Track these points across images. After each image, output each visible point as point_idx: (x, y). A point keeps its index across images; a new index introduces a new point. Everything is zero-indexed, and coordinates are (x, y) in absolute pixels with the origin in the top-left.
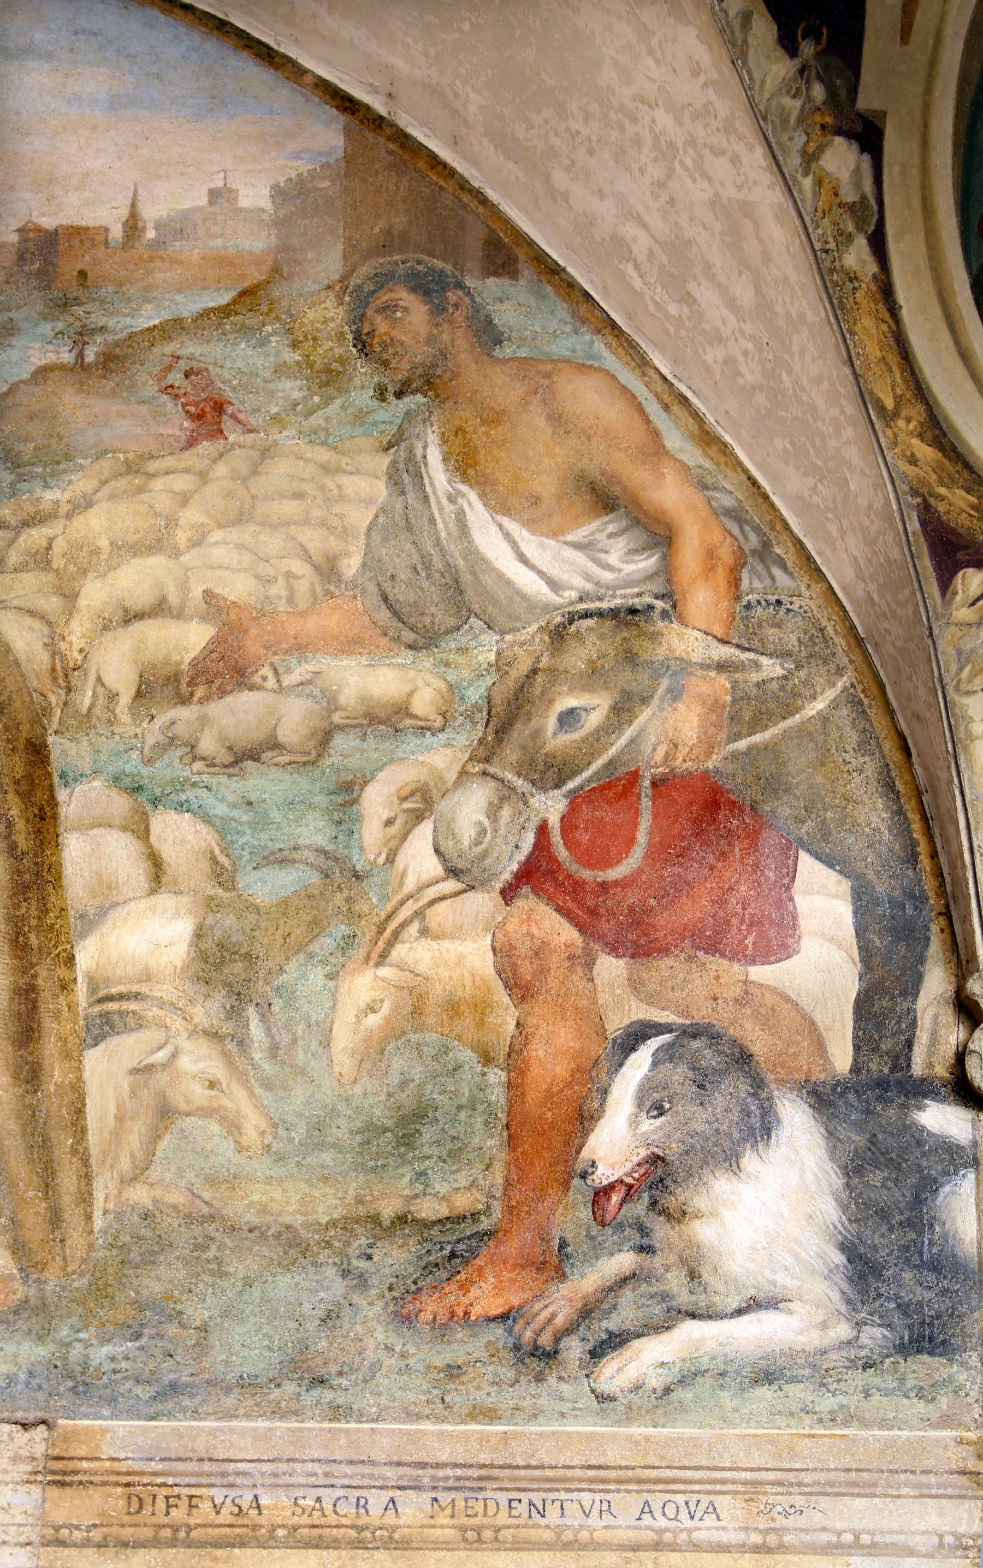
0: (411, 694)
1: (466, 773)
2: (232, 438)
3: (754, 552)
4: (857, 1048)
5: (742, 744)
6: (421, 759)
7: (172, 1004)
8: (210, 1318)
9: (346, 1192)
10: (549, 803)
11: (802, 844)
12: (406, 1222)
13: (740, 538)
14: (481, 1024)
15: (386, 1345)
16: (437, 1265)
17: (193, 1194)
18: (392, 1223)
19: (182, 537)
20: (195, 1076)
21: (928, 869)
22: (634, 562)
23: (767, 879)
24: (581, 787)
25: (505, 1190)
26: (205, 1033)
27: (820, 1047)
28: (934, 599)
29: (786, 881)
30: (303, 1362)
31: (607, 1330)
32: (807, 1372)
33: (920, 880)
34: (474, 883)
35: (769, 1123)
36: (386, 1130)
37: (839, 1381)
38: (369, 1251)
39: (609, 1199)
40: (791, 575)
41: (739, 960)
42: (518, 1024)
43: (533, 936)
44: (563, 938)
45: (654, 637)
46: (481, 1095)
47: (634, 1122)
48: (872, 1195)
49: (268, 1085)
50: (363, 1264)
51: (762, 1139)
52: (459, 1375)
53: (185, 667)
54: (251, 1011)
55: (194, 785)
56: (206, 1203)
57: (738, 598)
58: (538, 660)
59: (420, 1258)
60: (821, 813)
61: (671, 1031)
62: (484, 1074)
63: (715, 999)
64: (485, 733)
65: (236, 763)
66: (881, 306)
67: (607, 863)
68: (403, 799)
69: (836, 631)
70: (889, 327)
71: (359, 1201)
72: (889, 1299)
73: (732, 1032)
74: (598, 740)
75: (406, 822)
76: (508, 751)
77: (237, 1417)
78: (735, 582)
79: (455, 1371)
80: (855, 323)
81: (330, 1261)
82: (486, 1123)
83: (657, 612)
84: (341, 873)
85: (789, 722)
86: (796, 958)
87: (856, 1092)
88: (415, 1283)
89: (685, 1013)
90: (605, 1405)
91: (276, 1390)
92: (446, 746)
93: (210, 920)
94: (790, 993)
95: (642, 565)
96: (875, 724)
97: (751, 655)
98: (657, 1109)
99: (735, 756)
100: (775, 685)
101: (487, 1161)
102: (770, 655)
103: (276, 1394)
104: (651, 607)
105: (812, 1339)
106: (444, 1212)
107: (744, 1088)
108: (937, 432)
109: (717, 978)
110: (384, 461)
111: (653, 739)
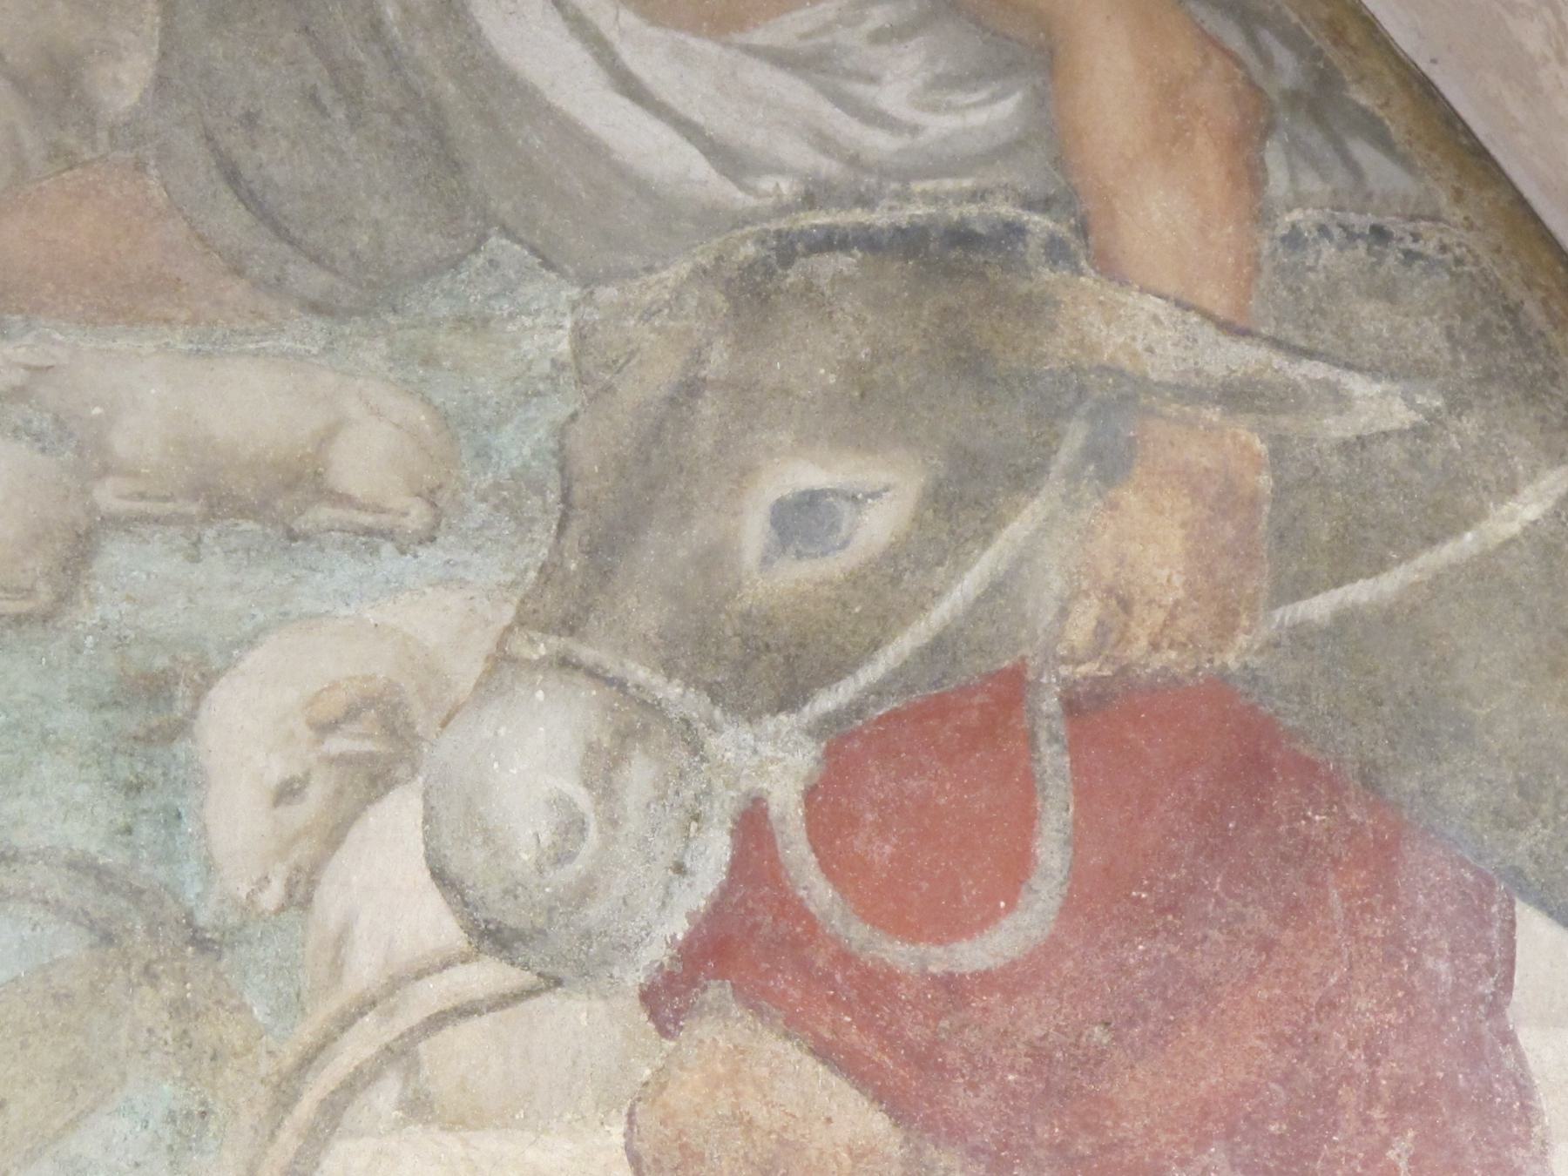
0: (328, 435)
1: (513, 660)
3: (1294, 98)
5: (1319, 607)
6: (371, 616)
10: (767, 750)
11: (1519, 884)
22: (951, 108)
23: (1432, 979)
24: (857, 709)
29: (1486, 987)
34: (563, 972)
40: (1404, 161)
43: (749, 1125)
45: (1035, 309)
57: (1262, 216)
58: (698, 357)
64: (557, 549)
68: (325, 728)
74: (895, 580)
75: (339, 792)
76: (632, 602)
78: (1252, 176)
83: (1033, 247)
84: (151, 931)
92: (444, 582)
95: (978, 118)
97: (1318, 370)
99: (1301, 638)
100: (1394, 452)
102: (1374, 371)
104: (1015, 231)
111: (1057, 583)
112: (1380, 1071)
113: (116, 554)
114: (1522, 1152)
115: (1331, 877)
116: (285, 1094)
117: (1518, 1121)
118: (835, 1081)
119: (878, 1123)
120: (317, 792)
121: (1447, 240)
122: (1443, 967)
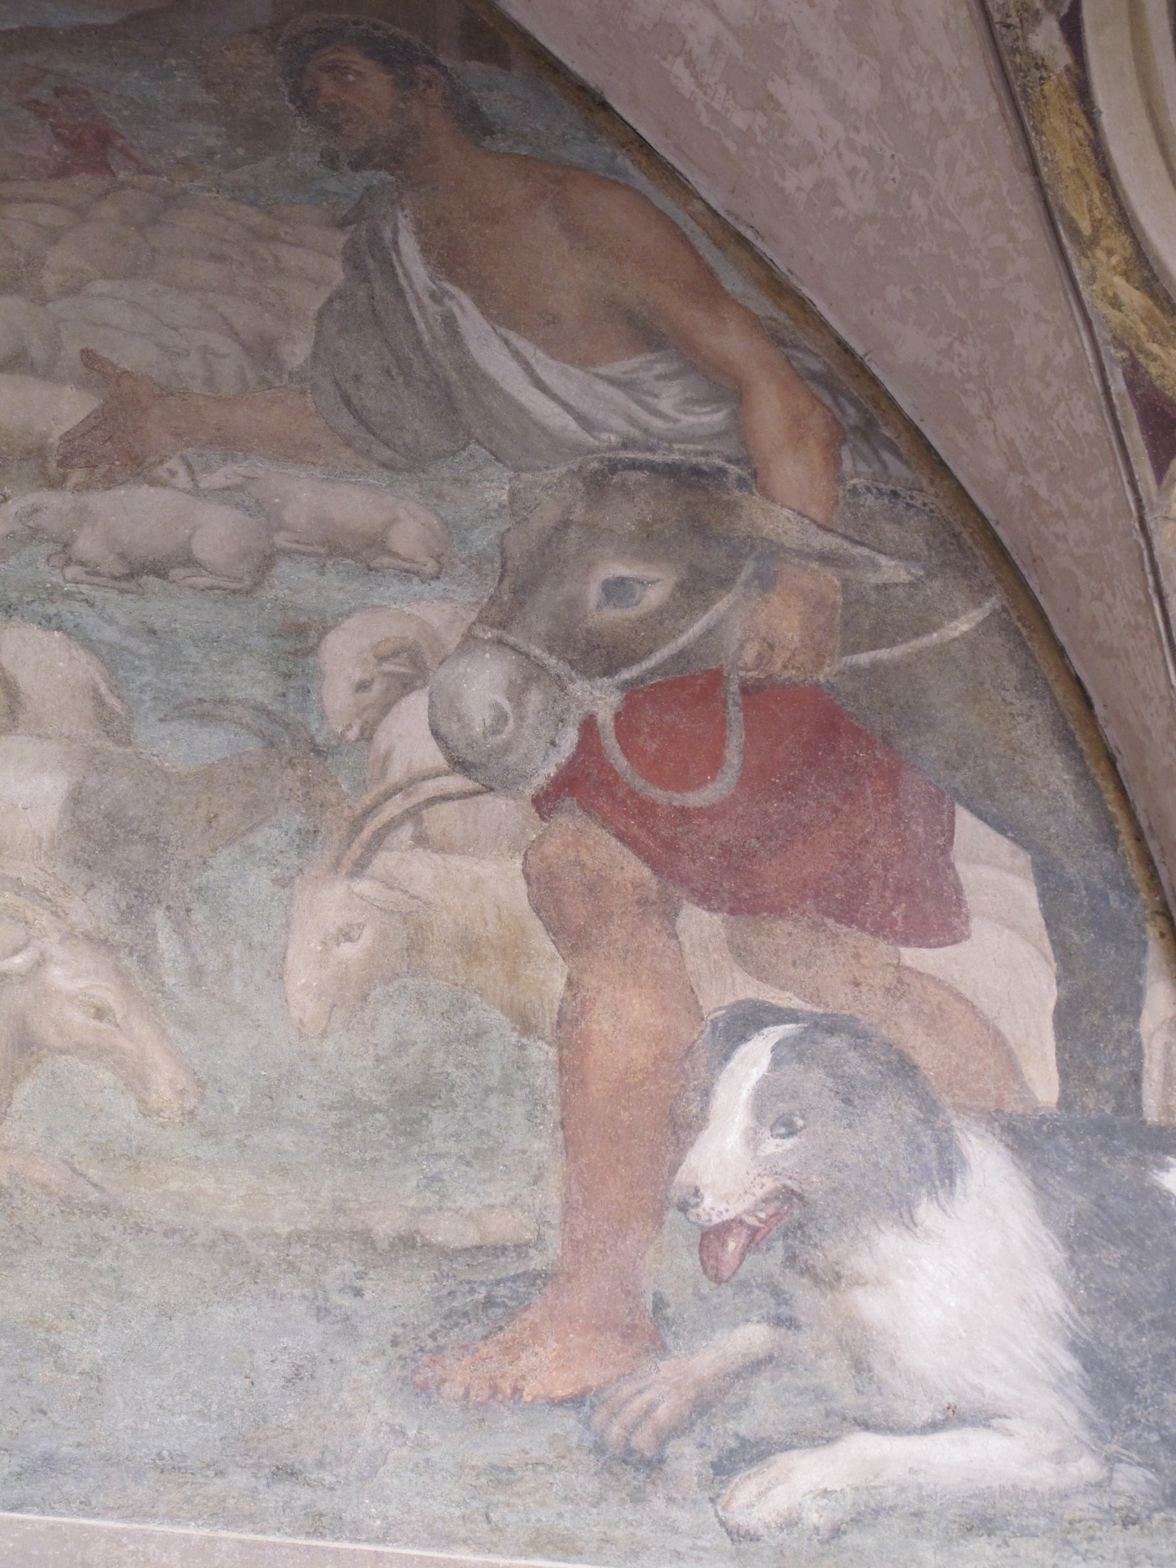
1: (475, 638)
2: (122, 175)
4: (1064, 1075)
5: (864, 659)
6: (407, 610)
7: (36, 890)
8: (104, 1358)
9: (317, 1193)
10: (597, 694)
11: (957, 796)
12: (414, 1247)
13: (836, 410)
14: (513, 977)
15: (392, 1427)
16: (465, 1314)
17: (74, 1170)
18: (392, 1245)
19: (50, 281)
20: (71, 998)
21: (1133, 852)
22: (693, 413)
23: (916, 834)
24: (641, 679)
25: (565, 1214)
26: (88, 937)
27: (1011, 1067)
28: (1146, 483)
30: (259, 1441)
31: (737, 1435)
32: (1042, 1522)
33: (1124, 866)
34: (493, 785)
35: (951, 1162)
36: (375, 1109)
37: (1091, 1539)
38: (358, 1283)
39: (724, 1244)
41: (885, 937)
42: (570, 983)
43: (583, 866)
44: (628, 874)
45: (731, 508)
46: (519, 1075)
47: (752, 1140)
48: (1108, 1279)
49: (189, 1025)
50: (347, 1302)
51: (943, 1185)
52: (509, 1483)
53: (54, 440)
54: (159, 916)
55: (68, 595)
56: (95, 1185)
57: (840, 480)
58: (569, 510)
59: (438, 1300)
60: (980, 761)
61: (796, 1020)
62: (523, 1047)
63: (857, 984)
64: (498, 589)
65: (131, 576)
66: (1075, 105)
67: (683, 783)
68: (383, 659)
69: (975, 540)
70: (1086, 133)
71: (339, 1208)
72: (1148, 1428)
73: (884, 1031)
74: (661, 623)
75: (388, 689)
76: (534, 618)
77: (155, 1516)
78: (837, 462)
79: (504, 1476)
80: (1042, 121)
81: (297, 1292)
82: (530, 1117)
83: (731, 480)
84: (293, 743)
85: (925, 641)
86: (966, 944)
87: (1070, 1134)
88: (433, 1337)
89: (815, 997)
90: (744, 1546)
91: (218, 1481)
92: (443, 598)
93: (92, 782)
94: (962, 989)
95: (706, 419)
96: (1040, 661)
97: (865, 552)
98: (784, 1125)
99: (855, 672)
100: (901, 593)
101: (535, 1170)
102: (891, 555)
103: (218, 1485)
104: (722, 472)
105: (1044, 1475)
106: (472, 1237)
107: (911, 1111)
108: (1146, 274)
109: (857, 956)
110: (340, 239)
111: (739, 633)
112: (889, 875)
113: (284, 567)
114: (957, 920)
115: (868, 783)
116: (356, 826)
117: (955, 905)
118: (626, 850)
119: (646, 872)
120: (377, 688)
121: (926, 501)
122: (920, 830)
